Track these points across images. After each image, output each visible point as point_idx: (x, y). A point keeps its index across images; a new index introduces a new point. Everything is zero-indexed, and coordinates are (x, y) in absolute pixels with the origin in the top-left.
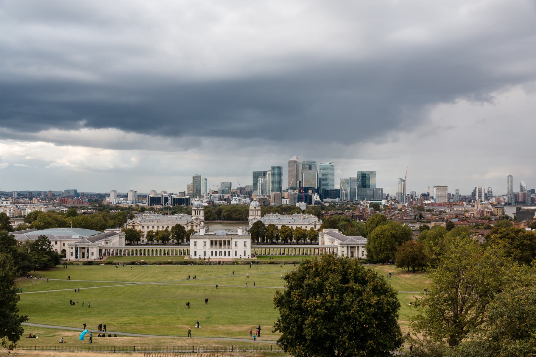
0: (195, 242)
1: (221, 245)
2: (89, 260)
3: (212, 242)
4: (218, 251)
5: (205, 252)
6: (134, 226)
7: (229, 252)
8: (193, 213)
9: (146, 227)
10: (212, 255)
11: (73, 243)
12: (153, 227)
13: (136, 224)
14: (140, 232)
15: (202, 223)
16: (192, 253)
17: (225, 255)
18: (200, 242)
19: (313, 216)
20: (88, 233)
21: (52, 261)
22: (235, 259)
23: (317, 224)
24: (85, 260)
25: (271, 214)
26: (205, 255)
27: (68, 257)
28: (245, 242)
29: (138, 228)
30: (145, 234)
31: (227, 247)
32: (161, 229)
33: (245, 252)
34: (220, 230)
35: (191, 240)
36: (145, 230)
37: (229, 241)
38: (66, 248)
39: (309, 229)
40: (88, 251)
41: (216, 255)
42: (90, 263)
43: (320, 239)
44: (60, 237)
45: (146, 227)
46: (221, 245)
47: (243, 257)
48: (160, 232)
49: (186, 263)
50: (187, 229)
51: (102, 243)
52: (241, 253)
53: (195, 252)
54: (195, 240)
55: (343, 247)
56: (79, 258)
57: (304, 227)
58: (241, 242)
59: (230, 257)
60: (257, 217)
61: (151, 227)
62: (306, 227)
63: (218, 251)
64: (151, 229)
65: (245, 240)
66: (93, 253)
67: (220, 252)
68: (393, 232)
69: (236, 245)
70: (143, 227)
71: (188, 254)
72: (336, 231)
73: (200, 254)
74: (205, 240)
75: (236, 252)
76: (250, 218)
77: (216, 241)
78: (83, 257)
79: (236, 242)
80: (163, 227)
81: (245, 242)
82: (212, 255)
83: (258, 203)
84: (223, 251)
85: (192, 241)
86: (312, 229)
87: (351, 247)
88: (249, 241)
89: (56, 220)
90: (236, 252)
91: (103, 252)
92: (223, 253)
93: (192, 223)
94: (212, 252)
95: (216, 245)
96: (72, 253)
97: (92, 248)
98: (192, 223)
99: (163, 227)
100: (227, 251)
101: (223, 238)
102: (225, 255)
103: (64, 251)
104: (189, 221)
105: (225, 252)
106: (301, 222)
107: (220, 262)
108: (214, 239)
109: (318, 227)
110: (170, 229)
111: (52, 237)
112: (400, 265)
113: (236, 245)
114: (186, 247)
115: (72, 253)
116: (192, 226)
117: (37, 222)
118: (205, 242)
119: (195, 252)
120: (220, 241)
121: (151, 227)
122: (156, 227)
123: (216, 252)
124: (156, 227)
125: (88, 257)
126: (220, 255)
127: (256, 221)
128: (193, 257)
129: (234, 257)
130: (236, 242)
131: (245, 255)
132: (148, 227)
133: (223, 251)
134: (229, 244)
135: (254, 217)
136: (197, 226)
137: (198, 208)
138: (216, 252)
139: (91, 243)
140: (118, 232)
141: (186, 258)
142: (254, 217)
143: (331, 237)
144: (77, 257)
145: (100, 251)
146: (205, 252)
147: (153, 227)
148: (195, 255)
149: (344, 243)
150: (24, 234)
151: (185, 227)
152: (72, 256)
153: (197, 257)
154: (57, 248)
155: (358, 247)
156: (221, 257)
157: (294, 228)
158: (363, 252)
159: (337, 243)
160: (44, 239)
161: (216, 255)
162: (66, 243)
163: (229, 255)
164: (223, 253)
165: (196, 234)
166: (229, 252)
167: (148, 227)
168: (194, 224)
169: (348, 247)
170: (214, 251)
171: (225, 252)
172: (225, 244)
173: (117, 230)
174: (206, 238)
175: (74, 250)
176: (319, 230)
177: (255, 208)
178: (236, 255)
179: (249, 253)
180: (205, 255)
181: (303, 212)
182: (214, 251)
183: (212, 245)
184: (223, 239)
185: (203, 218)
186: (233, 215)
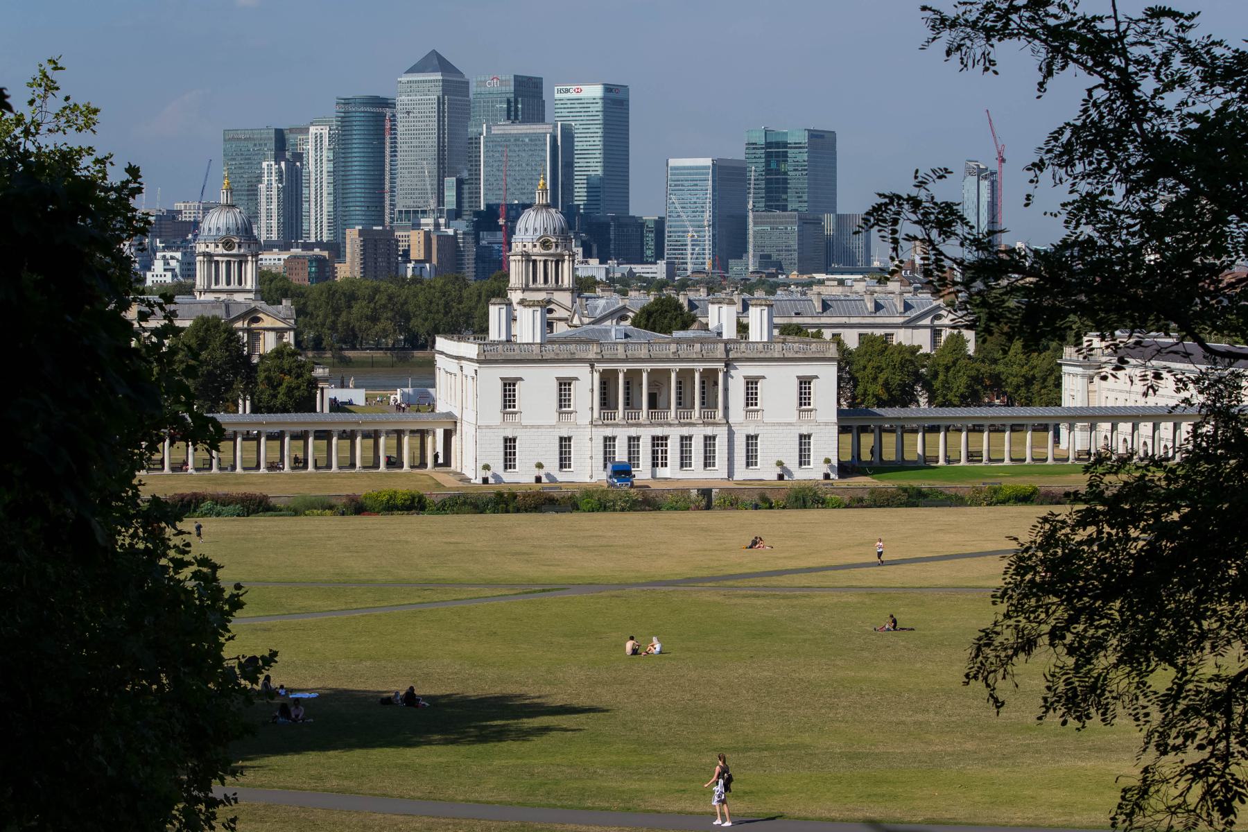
0: (509, 386)
3: (607, 382)
5: (565, 442)
7: (709, 440)
17: (685, 461)
18: (537, 384)
28: (805, 383)
33: (804, 439)
37: (709, 378)
52: (776, 451)
53: (510, 443)
54: (511, 371)
58: (779, 382)
59: (719, 470)
60: (557, 296)
65: (806, 370)
69: (751, 398)
74: (566, 371)
75: (751, 439)
77: (633, 378)
79: (751, 384)
81: (805, 383)
88: (826, 377)
90: (751, 439)
102: (685, 461)
105: (685, 440)
107: (706, 493)
113: (751, 398)
118: (564, 385)
119: (510, 443)
129: (741, 473)
130: (751, 384)
131: (804, 459)
137: (228, 245)
146: (565, 442)
148: (509, 462)
163: (708, 461)
166: (709, 440)
171: (685, 440)
177: (545, 244)
178: (751, 460)
179: (827, 445)
183: (607, 401)
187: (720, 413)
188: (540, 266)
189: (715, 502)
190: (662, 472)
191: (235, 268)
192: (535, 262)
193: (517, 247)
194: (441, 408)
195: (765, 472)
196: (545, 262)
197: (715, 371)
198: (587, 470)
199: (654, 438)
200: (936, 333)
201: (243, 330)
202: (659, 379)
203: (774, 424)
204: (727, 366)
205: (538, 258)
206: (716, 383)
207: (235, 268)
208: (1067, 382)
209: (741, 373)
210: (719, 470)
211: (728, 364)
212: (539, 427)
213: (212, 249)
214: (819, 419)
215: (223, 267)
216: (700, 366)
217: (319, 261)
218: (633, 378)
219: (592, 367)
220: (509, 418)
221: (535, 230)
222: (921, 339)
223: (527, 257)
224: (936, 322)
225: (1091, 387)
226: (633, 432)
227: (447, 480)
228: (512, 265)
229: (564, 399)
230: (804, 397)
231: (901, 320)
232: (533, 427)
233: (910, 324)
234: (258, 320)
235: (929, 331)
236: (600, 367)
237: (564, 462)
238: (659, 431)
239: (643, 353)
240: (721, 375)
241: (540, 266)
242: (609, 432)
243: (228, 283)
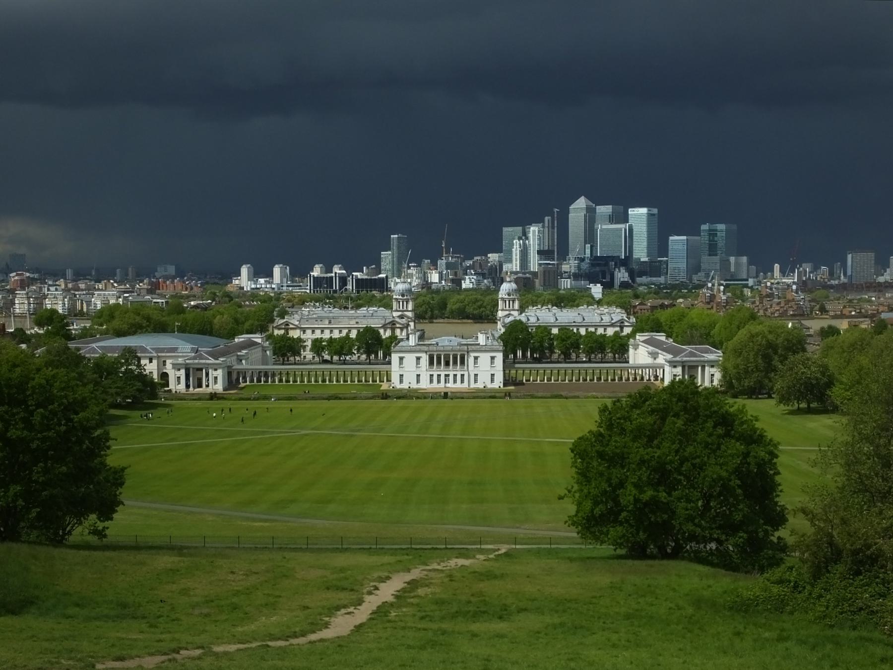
0: (401, 359)
1: (447, 364)
2: (210, 390)
4: (443, 374)
6: (287, 330)
7: (462, 376)
8: (395, 304)
9: (309, 332)
10: (431, 381)
11: (180, 360)
13: (291, 326)
14: (300, 340)
15: (412, 324)
16: (395, 379)
17: (455, 381)
18: (410, 358)
19: (619, 310)
20: (207, 343)
21: (146, 393)
22: (474, 389)
23: (626, 324)
24: (203, 390)
25: (539, 306)
27: (172, 386)
28: (493, 358)
29: (295, 334)
30: (309, 344)
32: (336, 335)
33: (493, 375)
34: (447, 339)
35: (393, 355)
36: (309, 336)
38: (169, 369)
39: (610, 332)
40: (207, 375)
41: (439, 382)
42: (213, 396)
44: (158, 350)
45: (309, 332)
46: (447, 364)
47: (490, 386)
48: (335, 339)
49: (385, 396)
51: (231, 360)
53: (401, 376)
54: (402, 355)
55: (675, 367)
56: (191, 389)
57: (600, 331)
58: (484, 358)
59: (465, 385)
60: (512, 312)
62: (605, 330)
63: (443, 374)
64: (318, 335)
66: (216, 378)
68: (770, 337)
70: (304, 332)
71: (389, 380)
72: (661, 337)
73: (409, 383)
75: (476, 375)
76: (500, 314)
78: (200, 386)
79: (476, 358)
81: (493, 358)
82: (431, 381)
83: (514, 286)
84: (452, 374)
85: (395, 357)
86: (616, 333)
87: (691, 367)
88: (499, 357)
89: (148, 319)
90: (476, 375)
91: (234, 376)
92: (451, 378)
93: (393, 323)
94: (432, 376)
95: (439, 363)
96: (179, 378)
97: (216, 370)
99: (340, 332)
100: (459, 374)
102: (455, 381)
103: (164, 376)
105: (455, 376)
107: (446, 394)
109: (627, 330)
110: (353, 335)
111: (144, 350)
112: (784, 399)
114: (384, 367)
115: (179, 378)
116: (393, 330)
117: (116, 323)
118: (418, 359)
119: (401, 376)
121: (318, 332)
122: (327, 332)
123: (439, 376)
125: (207, 386)
127: (511, 319)
128: (399, 386)
129: (473, 385)
130: (476, 358)
131: (492, 381)
132: (313, 332)
133: (452, 374)
134: (462, 363)
135: (507, 312)
136: (402, 329)
137: (403, 295)
138: (439, 376)
139: (212, 361)
140: (259, 341)
142: (507, 312)
143: (651, 348)
144: (188, 386)
145: (230, 374)
146: (418, 376)
147: (322, 332)
148: (401, 381)
149: (678, 359)
150: (94, 345)
151: (382, 331)
152: (179, 383)
153: (405, 386)
154: (151, 368)
155: (703, 368)
157: (583, 331)
158: (713, 375)
159: (661, 359)
160: (131, 354)
161: (439, 382)
162: (169, 362)
163: (462, 381)
164: (451, 378)
165: (401, 344)
166: (462, 376)
169: (683, 367)
170: (435, 374)
171: (455, 376)
172: (455, 363)
173: (257, 338)
174: (420, 351)
175: (183, 372)
176: (629, 336)
177: (509, 295)
178: (476, 381)
180: (418, 381)
181: (599, 303)
182: (435, 374)
183: (431, 363)
186: (469, 310)
190: (448, 385)
193: (500, 296)
195: (480, 385)
198: (425, 384)
202: (447, 357)
209: (473, 355)
210: (465, 385)
211: (468, 352)
217: (526, 278)
223: (503, 299)
227: (385, 386)
230: (492, 363)
237: (418, 381)
238: (447, 373)
239: (442, 349)
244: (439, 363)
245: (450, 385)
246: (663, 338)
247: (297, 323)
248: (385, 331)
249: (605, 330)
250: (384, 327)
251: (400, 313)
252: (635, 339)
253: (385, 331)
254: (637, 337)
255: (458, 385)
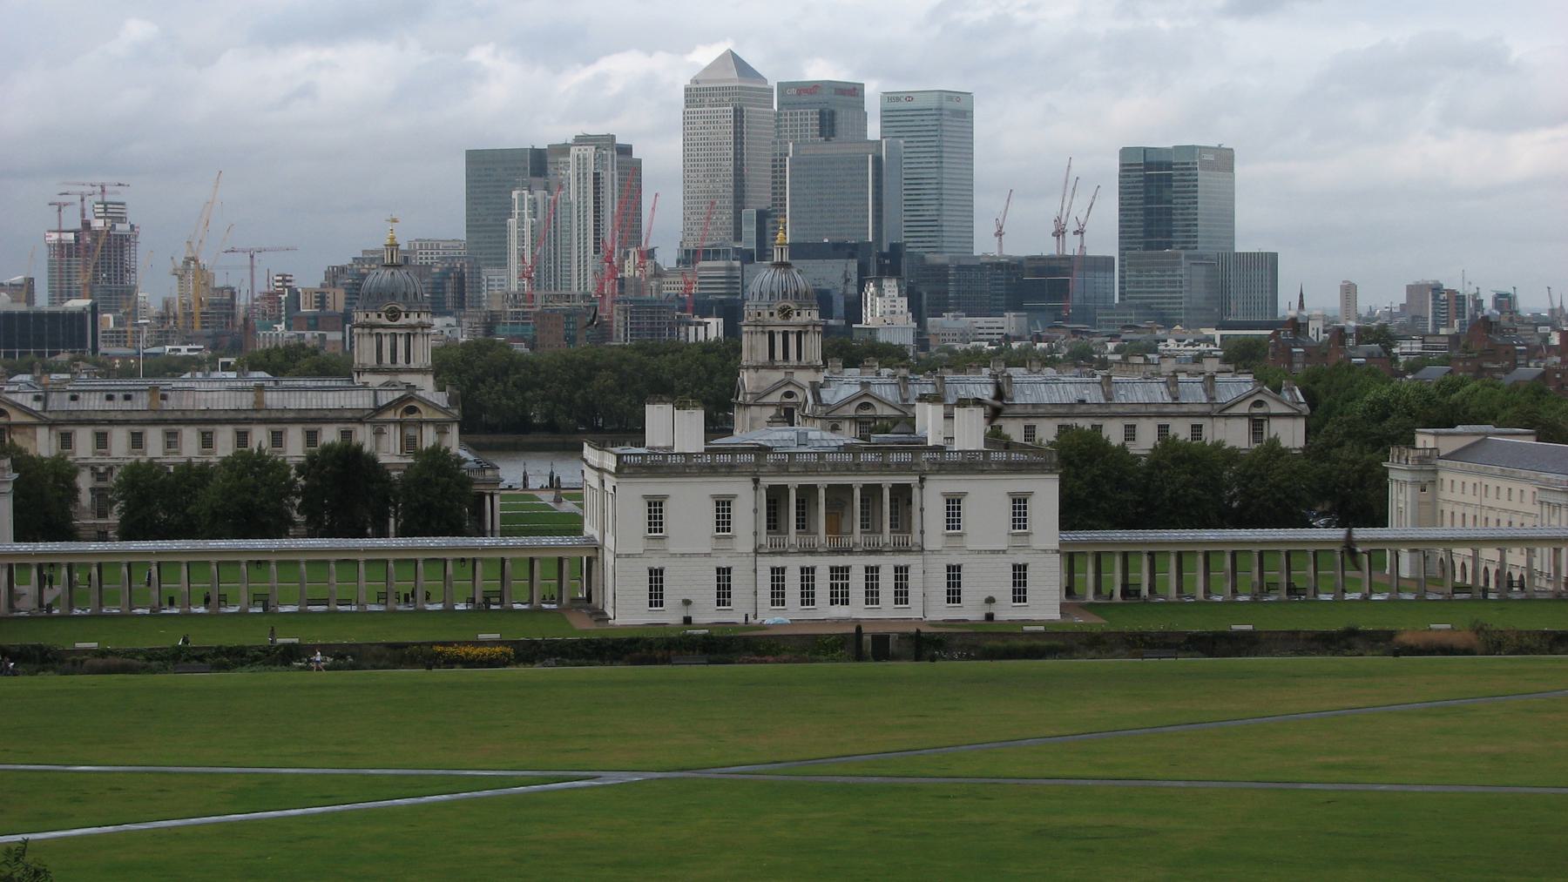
0: (655, 507)
1: (834, 528)
3: (776, 499)
5: (724, 574)
7: (901, 573)
8: (365, 352)
9: (84, 440)
10: (778, 596)
12: (137, 441)
13: (16, 417)
17: (872, 595)
18: (690, 503)
23: (1275, 408)
26: (723, 596)
28: (1019, 504)
29: (43, 445)
31: (887, 536)
33: (1020, 572)
37: (902, 495)
41: (808, 597)
43: (1401, 497)
45: (84, 440)
47: (1007, 612)
50: (389, 451)
53: (656, 576)
54: (655, 487)
58: (987, 498)
61: (119, 439)
62: (1196, 429)
63: (823, 565)
65: (1020, 483)
67: (840, 573)
70: (66, 441)
73: (692, 601)
74: (723, 486)
75: (954, 572)
79: (954, 505)
80: (207, 441)
81: (1019, 504)
82: (778, 596)
84: (857, 565)
88: (1045, 493)
90: (954, 572)
94: (778, 574)
98: (408, 403)
99: (207, 441)
101: (857, 468)
102: (872, 595)
104: (386, 398)
105: (872, 573)
106: (1159, 393)
108: (793, 482)
118: (723, 507)
119: (656, 576)
120: (838, 496)
121: (119, 439)
122: (154, 440)
123: (807, 574)
124: (154, 440)
126: (839, 595)
130: (954, 505)
131: (1020, 594)
132: (102, 441)
135: (779, 376)
138: (807, 574)
141: (581, 626)
142: (779, 376)
146: (724, 574)
147: (137, 441)
148: (656, 598)
151: (363, 436)
153: (670, 616)
156: (839, 611)
161: (808, 597)
163: (901, 595)
166: (901, 573)
167: (102, 441)
168: (426, 414)
170: (793, 566)
171: (872, 573)
174: (731, 470)
176: (1316, 448)
178: (954, 595)
180: (723, 596)
182: (793, 566)
183: (774, 522)
184: (857, 481)
185: (426, 386)
187: (916, 537)
188: (779, 340)
189: (892, 647)
191: (401, 343)
192: (772, 335)
194: (590, 529)
195: (970, 610)
196: (785, 334)
197: (907, 488)
198: (752, 607)
199: (832, 569)
200: (1257, 424)
201: (394, 422)
203: (979, 552)
204: (922, 480)
205: (775, 329)
206: (910, 502)
207: (401, 343)
208: (1393, 489)
210: (913, 611)
212: (690, 555)
213: (373, 318)
214: (1036, 545)
215: (387, 342)
216: (887, 481)
218: (806, 493)
219: (756, 481)
220: (654, 545)
221: (772, 294)
222: (1234, 435)
224: (1255, 410)
225: (1426, 496)
226: (808, 561)
228: (744, 337)
229: (723, 521)
231: (1207, 409)
232: (683, 555)
233: (1222, 412)
234: (412, 410)
235: (1244, 424)
236: (766, 481)
238: (840, 561)
240: (916, 491)
241: (779, 340)
242: (778, 562)
243: (394, 359)
244: (802, 524)
245: (856, 609)
246: (1531, 441)
247: (37, 406)
248: (379, 433)
249: (1196, 429)
250: (373, 417)
251: (384, 379)
252: (1411, 443)
253: (379, 433)
254: (1425, 439)
255: (887, 609)
